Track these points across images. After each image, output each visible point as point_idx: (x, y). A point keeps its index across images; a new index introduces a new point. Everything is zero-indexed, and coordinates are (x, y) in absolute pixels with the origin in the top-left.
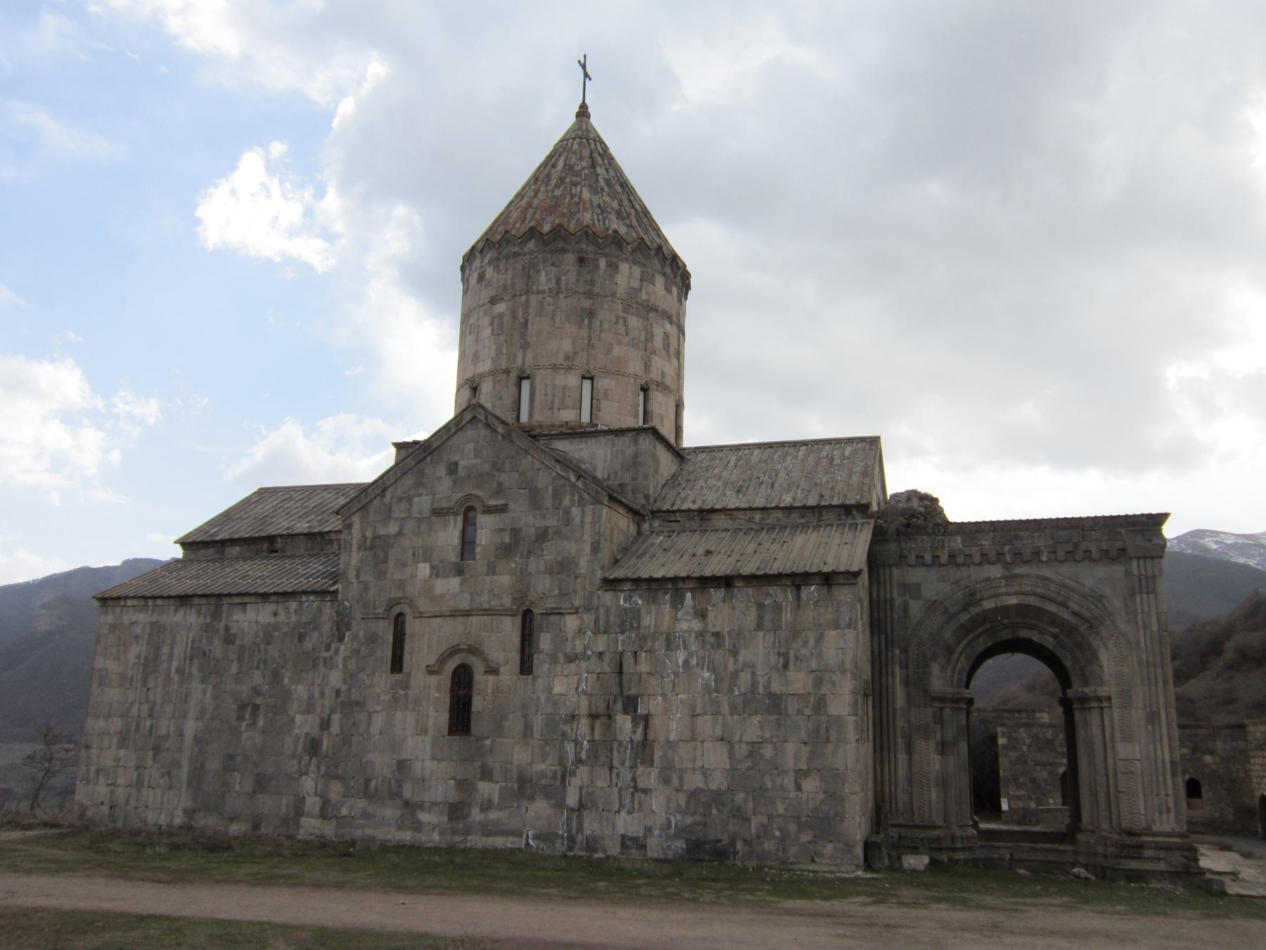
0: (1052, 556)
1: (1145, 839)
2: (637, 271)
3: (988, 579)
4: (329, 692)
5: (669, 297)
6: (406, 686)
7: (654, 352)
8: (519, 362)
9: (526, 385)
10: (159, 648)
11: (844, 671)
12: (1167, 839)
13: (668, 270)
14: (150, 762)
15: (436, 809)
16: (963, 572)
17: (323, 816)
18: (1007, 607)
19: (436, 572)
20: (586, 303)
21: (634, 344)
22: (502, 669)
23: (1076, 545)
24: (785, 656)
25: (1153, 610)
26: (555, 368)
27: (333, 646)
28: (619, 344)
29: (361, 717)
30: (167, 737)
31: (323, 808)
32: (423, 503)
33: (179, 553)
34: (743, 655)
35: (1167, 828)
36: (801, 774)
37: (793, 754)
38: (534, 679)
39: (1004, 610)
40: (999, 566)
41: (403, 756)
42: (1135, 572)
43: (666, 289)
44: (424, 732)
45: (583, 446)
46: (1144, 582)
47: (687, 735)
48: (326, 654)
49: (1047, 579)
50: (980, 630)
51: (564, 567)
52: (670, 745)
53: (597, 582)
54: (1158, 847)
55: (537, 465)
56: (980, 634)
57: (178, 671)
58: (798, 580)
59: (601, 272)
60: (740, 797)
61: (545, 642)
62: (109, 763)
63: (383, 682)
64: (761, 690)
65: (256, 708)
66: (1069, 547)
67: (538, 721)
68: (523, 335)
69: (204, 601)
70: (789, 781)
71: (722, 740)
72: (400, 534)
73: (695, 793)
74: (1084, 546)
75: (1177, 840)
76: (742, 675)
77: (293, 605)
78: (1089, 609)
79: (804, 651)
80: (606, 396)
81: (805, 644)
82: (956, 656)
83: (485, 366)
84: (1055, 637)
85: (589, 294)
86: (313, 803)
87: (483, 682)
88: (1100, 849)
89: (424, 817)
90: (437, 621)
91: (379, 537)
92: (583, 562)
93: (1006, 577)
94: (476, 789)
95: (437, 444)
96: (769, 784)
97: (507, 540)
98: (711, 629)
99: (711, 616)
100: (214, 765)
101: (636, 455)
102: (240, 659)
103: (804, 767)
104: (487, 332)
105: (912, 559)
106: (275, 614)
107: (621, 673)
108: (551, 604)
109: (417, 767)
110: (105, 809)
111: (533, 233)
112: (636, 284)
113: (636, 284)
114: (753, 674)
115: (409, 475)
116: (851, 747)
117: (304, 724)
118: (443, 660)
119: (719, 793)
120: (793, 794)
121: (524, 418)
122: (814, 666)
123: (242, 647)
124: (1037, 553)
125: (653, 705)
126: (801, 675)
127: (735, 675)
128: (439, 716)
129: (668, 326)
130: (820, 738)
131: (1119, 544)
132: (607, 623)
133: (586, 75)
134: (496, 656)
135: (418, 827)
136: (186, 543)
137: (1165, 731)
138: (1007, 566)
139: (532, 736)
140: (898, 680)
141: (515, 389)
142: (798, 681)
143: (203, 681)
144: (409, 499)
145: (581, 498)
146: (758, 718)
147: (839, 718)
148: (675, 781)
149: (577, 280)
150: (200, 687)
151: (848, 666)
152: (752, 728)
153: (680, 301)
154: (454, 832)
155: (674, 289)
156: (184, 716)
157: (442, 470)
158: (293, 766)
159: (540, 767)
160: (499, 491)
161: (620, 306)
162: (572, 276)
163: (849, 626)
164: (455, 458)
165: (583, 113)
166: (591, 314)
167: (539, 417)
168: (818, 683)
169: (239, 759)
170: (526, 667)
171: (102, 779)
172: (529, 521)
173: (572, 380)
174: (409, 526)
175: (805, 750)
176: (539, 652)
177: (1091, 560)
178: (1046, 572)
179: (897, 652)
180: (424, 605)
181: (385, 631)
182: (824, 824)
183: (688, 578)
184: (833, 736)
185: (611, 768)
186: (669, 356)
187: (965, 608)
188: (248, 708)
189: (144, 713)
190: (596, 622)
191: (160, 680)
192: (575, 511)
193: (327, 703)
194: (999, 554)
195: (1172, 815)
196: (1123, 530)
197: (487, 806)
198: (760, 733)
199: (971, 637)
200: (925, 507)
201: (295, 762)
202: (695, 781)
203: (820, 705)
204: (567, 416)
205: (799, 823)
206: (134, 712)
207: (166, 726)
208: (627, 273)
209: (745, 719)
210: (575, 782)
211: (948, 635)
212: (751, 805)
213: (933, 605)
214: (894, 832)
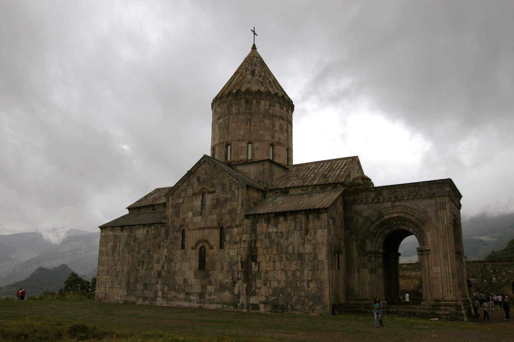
0: (409, 197)
1: (442, 302)
2: (268, 103)
3: (386, 208)
4: (164, 257)
5: (282, 111)
6: (185, 254)
7: (276, 131)
8: (226, 139)
9: (229, 147)
10: (116, 243)
11: (323, 244)
12: (450, 302)
13: (281, 101)
14: (115, 280)
15: (195, 295)
16: (377, 205)
17: (163, 297)
18: (394, 218)
19: (194, 215)
20: (249, 117)
21: (267, 129)
22: (215, 247)
23: (417, 193)
24: (304, 239)
25: (445, 216)
26: (238, 140)
27: (165, 241)
28: (261, 130)
29: (173, 264)
30: (119, 272)
31: (163, 295)
32: (190, 191)
33: (127, 212)
34: (290, 239)
35: (450, 298)
36: (309, 281)
37: (307, 274)
38: (224, 251)
39: (393, 219)
40: (390, 203)
41: (185, 278)
42: (439, 202)
44: (191, 269)
45: (247, 168)
46: (442, 205)
47: (272, 269)
48: (162, 244)
49: (407, 206)
50: (386, 227)
51: (233, 211)
52: (267, 272)
53: (243, 216)
54: (446, 305)
55: (224, 176)
56: (386, 228)
57: (122, 250)
58: (308, 212)
59: (254, 105)
60: (289, 290)
61: (227, 238)
62: (104, 280)
63: (179, 252)
64: (296, 252)
65: (143, 262)
66: (415, 194)
67: (226, 265)
68: (228, 130)
69: (128, 227)
70: (305, 284)
72: (183, 202)
73: (275, 288)
74: (420, 193)
75: (454, 303)
76: (290, 247)
77: (153, 228)
78: (422, 217)
79: (310, 237)
80: (257, 149)
81: (310, 235)
82: (377, 237)
83: (217, 142)
85: (250, 113)
86: (160, 293)
87: (209, 252)
88: (427, 307)
89: (192, 297)
90: (194, 232)
91: (177, 204)
92: (239, 209)
93: (392, 207)
94: (207, 288)
95: (193, 171)
96: (299, 285)
97: (215, 203)
98: (280, 231)
99: (280, 226)
100: (132, 280)
101: (264, 170)
102: (139, 246)
103: (310, 279)
104: (217, 130)
105: (359, 201)
108: (229, 224)
109: (189, 281)
110: (103, 295)
111: (230, 93)
112: (268, 108)
113: (268, 108)
114: (293, 246)
115: (186, 182)
116: (326, 271)
117: (157, 267)
118: (196, 245)
119: (282, 288)
120: (307, 288)
121: (229, 159)
122: (313, 242)
123: (139, 242)
124: (404, 196)
126: (309, 246)
127: (287, 247)
128: (196, 264)
129: (282, 121)
130: (315, 269)
131: (433, 191)
132: (247, 230)
133: (255, 34)
134: (213, 243)
135: (190, 301)
136: (129, 208)
137: (449, 262)
138: (393, 202)
139: (224, 270)
141: (225, 149)
142: (308, 248)
143: (129, 254)
144: (186, 190)
145: (238, 186)
146: (295, 262)
147: (322, 262)
148: (268, 285)
149: (246, 109)
150: (128, 255)
151: (325, 242)
152: (294, 266)
153: (288, 111)
154: (201, 303)
155: (285, 108)
156: (124, 265)
157: (195, 180)
158: (154, 281)
159: (226, 280)
160: (213, 185)
161: (261, 116)
162: (244, 107)
163: (325, 228)
164: (199, 175)
165: (254, 47)
166: (250, 120)
167: (233, 159)
168: (315, 249)
169: (139, 279)
170: (221, 246)
171: (102, 285)
172: (222, 196)
173: (244, 144)
174: (186, 199)
175: (311, 273)
176: (225, 241)
177: (423, 198)
178: (408, 204)
179: (354, 236)
180: (191, 226)
181: (179, 235)
182: (317, 299)
183: (271, 213)
184: (320, 267)
186: (283, 132)
187: (378, 219)
188: (141, 262)
189: (113, 264)
190: (243, 229)
191: (117, 253)
193: (163, 260)
194: (389, 198)
195: (452, 293)
196: (434, 186)
197: (210, 294)
198: (295, 267)
199: (382, 229)
200: (364, 182)
201: (154, 280)
202: (275, 284)
203: (315, 257)
204: (243, 157)
205: (309, 299)
206: (110, 264)
207: (119, 268)
208: (264, 104)
209: (290, 263)
211: (372, 229)
212: (293, 293)
213: (367, 218)
214: (353, 302)
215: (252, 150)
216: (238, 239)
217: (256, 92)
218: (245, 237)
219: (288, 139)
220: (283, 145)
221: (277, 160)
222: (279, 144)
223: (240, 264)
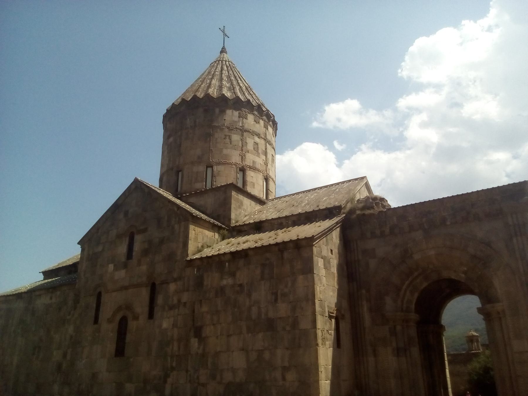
2: (236, 113)
5: (257, 125)
9: (180, 174)
19: (116, 268)
24: (276, 294)
32: (114, 233)
33: (42, 277)
36: (285, 369)
43: (255, 121)
48: (68, 317)
50: (416, 274)
52: (217, 354)
61: (160, 300)
64: (263, 316)
70: (278, 374)
71: (243, 350)
77: (58, 293)
84: (465, 273)
87: (132, 325)
98: (239, 283)
99: (238, 274)
103: (286, 364)
104: (166, 153)
106: (51, 298)
107: (194, 311)
113: (236, 119)
117: (57, 355)
125: (208, 331)
128: (111, 347)
129: (257, 139)
133: (225, 35)
136: (47, 274)
140: (365, 309)
146: (260, 335)
155: (262, 122)
157: (121, 216)
165: (223, 51)
170: (151, 315)
179: (364, 291)
181: (92, 301)
185: (187, 371)
192: (176, 227)
199: (410, 279)
202: (228, 377)
203: (295, 324)
204: (199, 186)
210: (169, 380)
215: (212, 176)
216: (175, 301)
217: (218, 98)
218: (185, 297)
219: (266, 164)
220: (259, 171)
221: (249, 189)
222: (254, 168)
223: (176, 344)
